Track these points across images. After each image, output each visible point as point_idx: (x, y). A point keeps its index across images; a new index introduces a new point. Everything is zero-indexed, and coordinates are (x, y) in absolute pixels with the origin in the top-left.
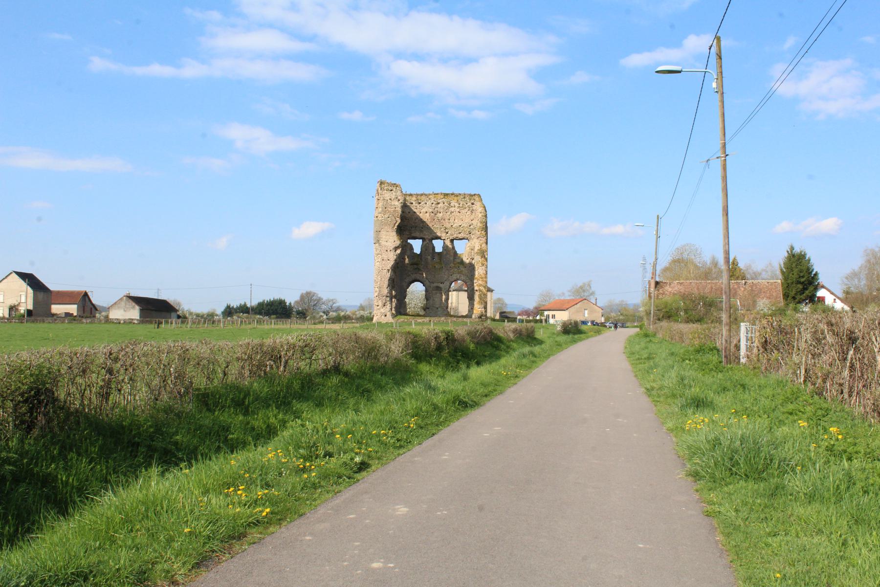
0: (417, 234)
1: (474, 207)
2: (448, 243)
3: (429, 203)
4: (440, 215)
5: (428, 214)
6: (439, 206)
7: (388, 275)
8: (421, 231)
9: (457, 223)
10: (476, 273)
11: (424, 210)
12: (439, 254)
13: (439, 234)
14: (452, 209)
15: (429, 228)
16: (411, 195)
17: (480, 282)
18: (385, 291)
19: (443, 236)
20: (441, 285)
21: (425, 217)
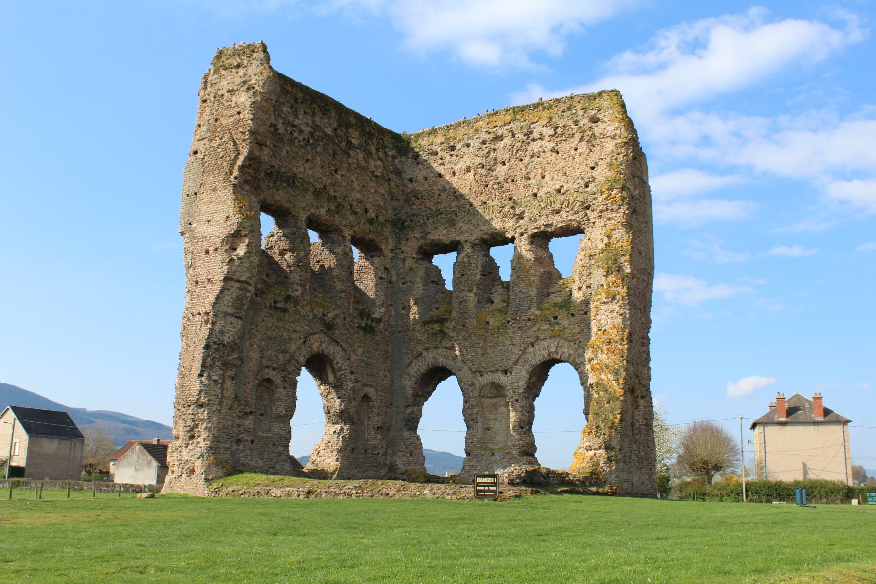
0: (442, 235)
1: (598, 129)
2: (523, 245)
3: (475, 143)
4: (501, 171)
5: (470, 175)
6: (501, 145)
7: (205, 332)
8: (452, 223)
9: (549, 186)
10: (594, 329)
11: (462, 165)
12: (506, 286)
13: (497, 224)
14: (535, 147)
15: (469, 209)
16: (433, 132)
17: (603, 357)
18: (195, 386)
19: (509, 226)
20: (503, 379)
21: (464, 183)
